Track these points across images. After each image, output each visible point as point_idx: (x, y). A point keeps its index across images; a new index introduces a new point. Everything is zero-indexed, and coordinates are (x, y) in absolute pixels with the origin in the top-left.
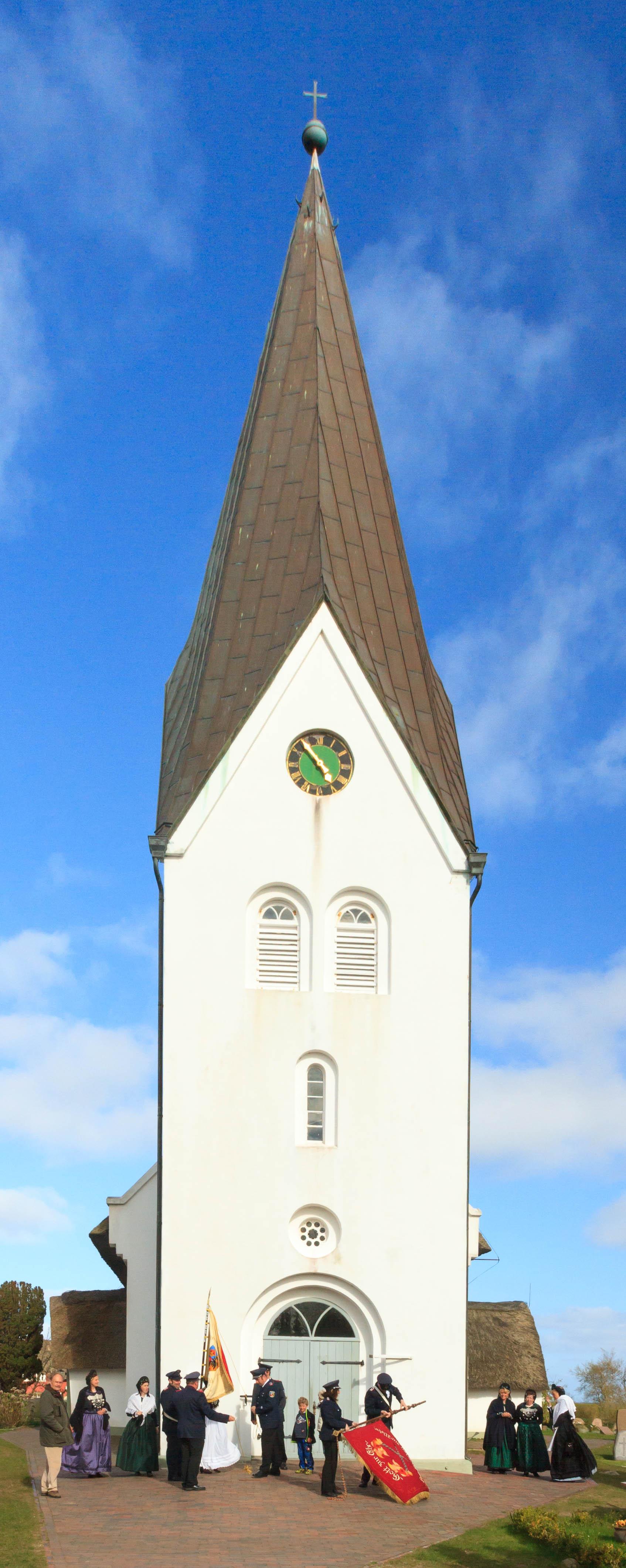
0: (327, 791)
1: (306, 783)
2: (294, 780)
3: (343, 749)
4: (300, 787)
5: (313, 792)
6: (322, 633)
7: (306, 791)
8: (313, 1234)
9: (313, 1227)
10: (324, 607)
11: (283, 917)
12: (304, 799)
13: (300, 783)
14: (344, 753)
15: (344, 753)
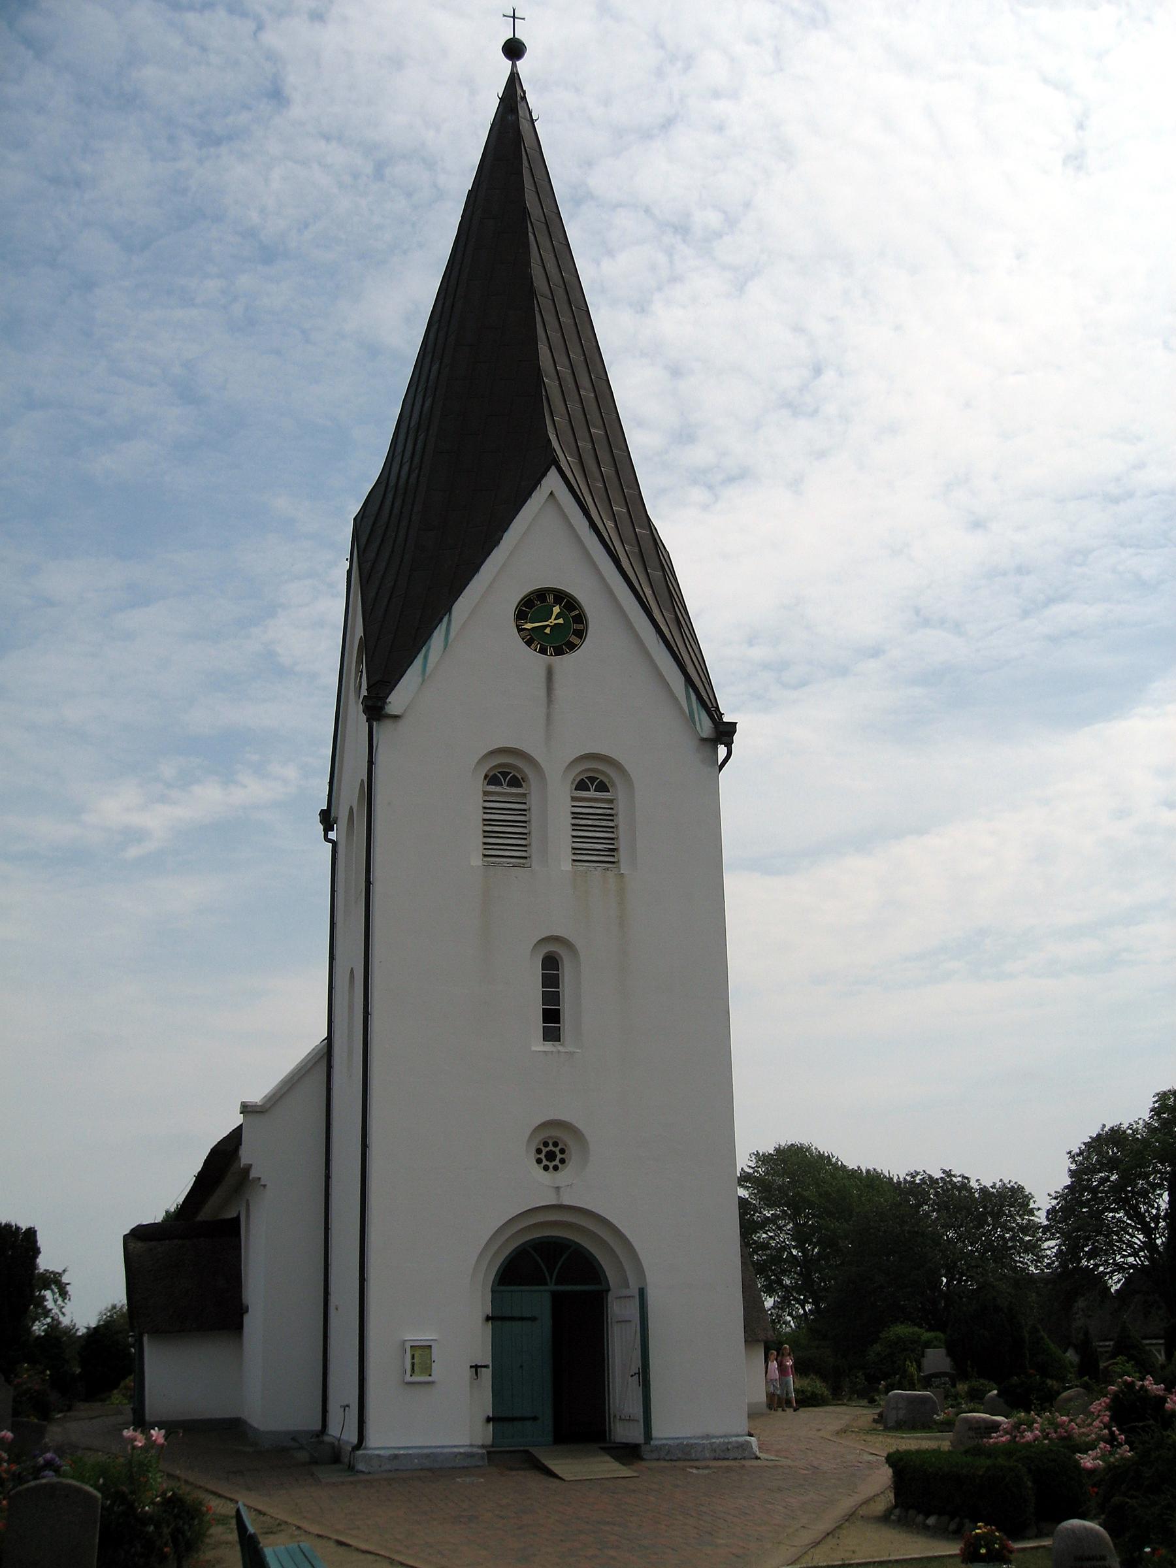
0: (559, 652)
1: (536, 643)
2: (523, 639)
3: (576, 609)
4: (529, 646)
5: (543, 651)
6: (551, 493)
7: (535, 650)
8: (551, 1156)
9: (551, 1147)
10: (553, 468)
11: (509, 785)
12: (533, 661)
13: (529, 643)
14: (576, 612)
15: (576, 612)
